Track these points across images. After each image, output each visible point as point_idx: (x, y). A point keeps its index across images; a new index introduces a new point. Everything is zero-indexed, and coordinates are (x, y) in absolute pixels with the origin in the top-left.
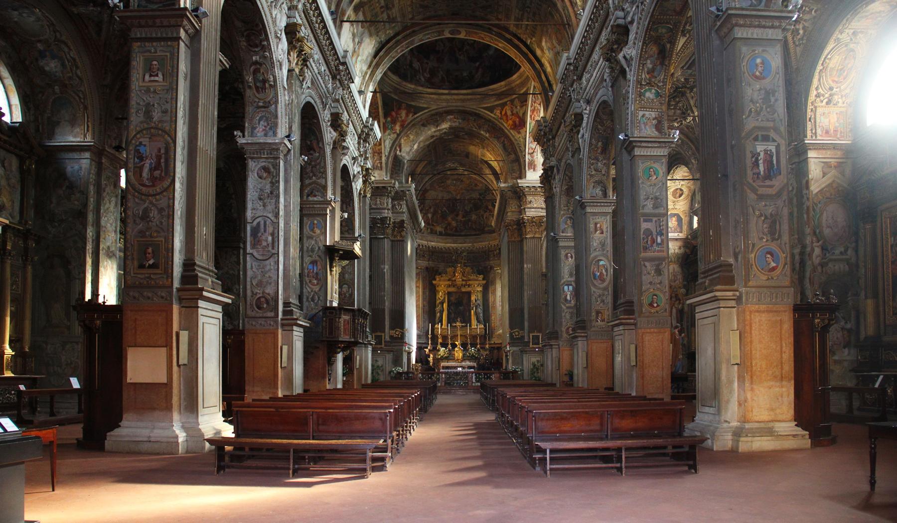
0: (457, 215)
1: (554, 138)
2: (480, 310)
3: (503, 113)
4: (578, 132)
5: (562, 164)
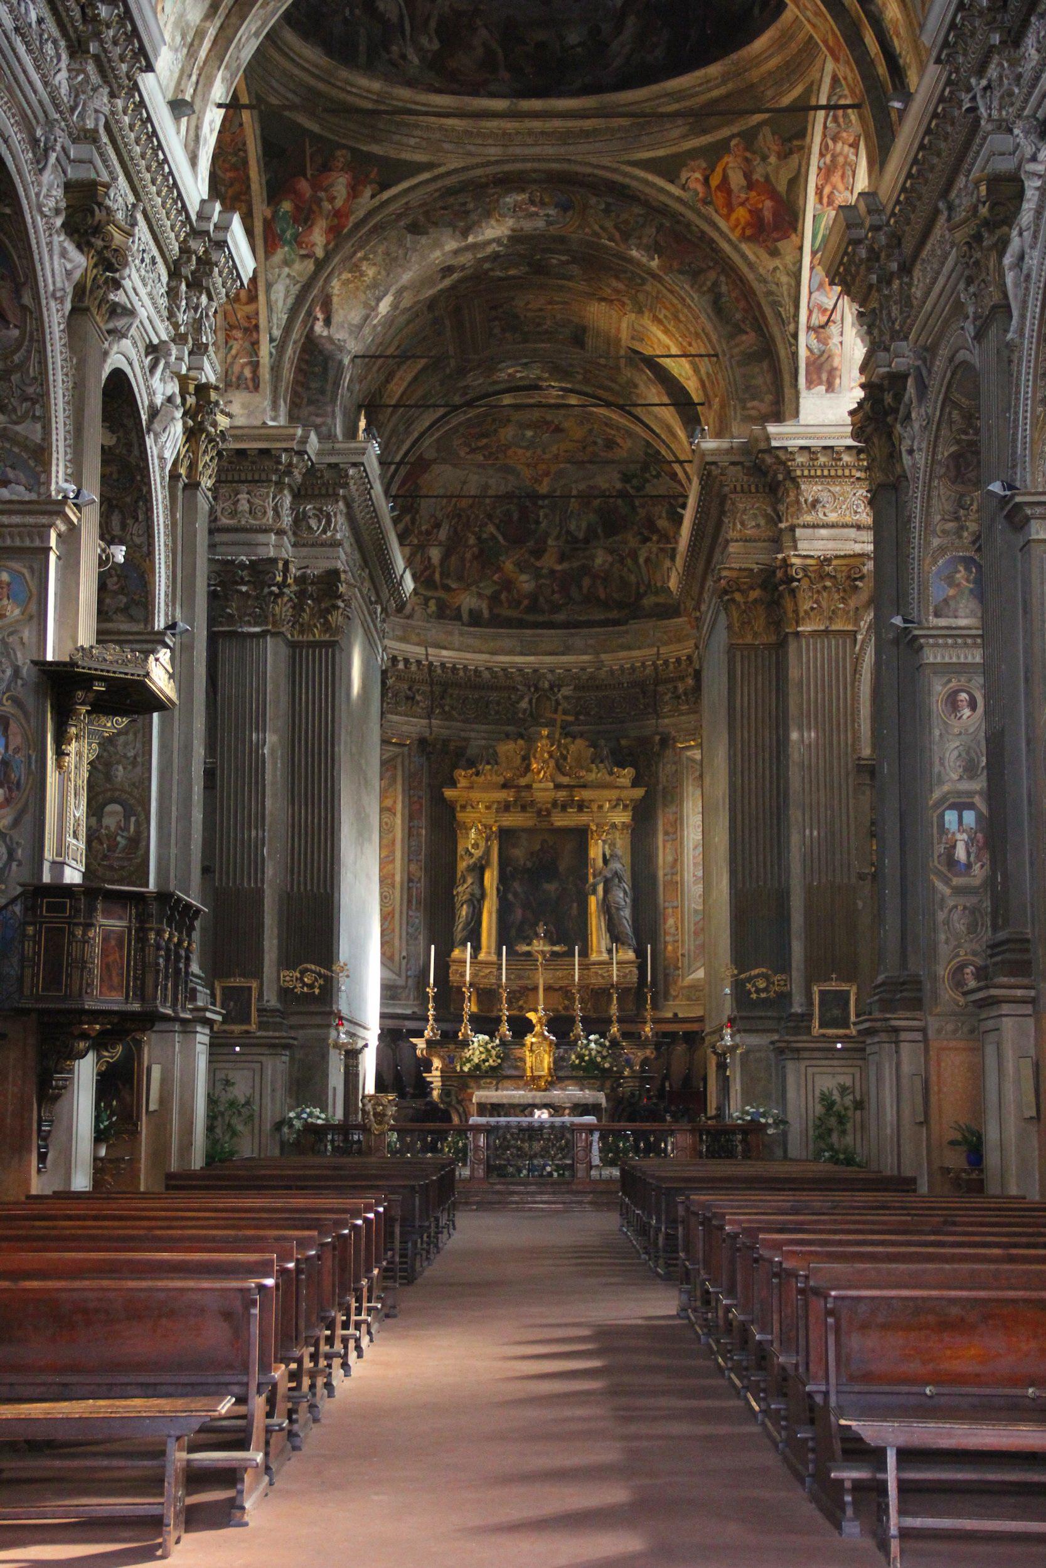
0: (538, 553)
1: (906, 269)
2: (621, 896)
3: (715, 182)
4: (1002, 245)
5: (939, 364)
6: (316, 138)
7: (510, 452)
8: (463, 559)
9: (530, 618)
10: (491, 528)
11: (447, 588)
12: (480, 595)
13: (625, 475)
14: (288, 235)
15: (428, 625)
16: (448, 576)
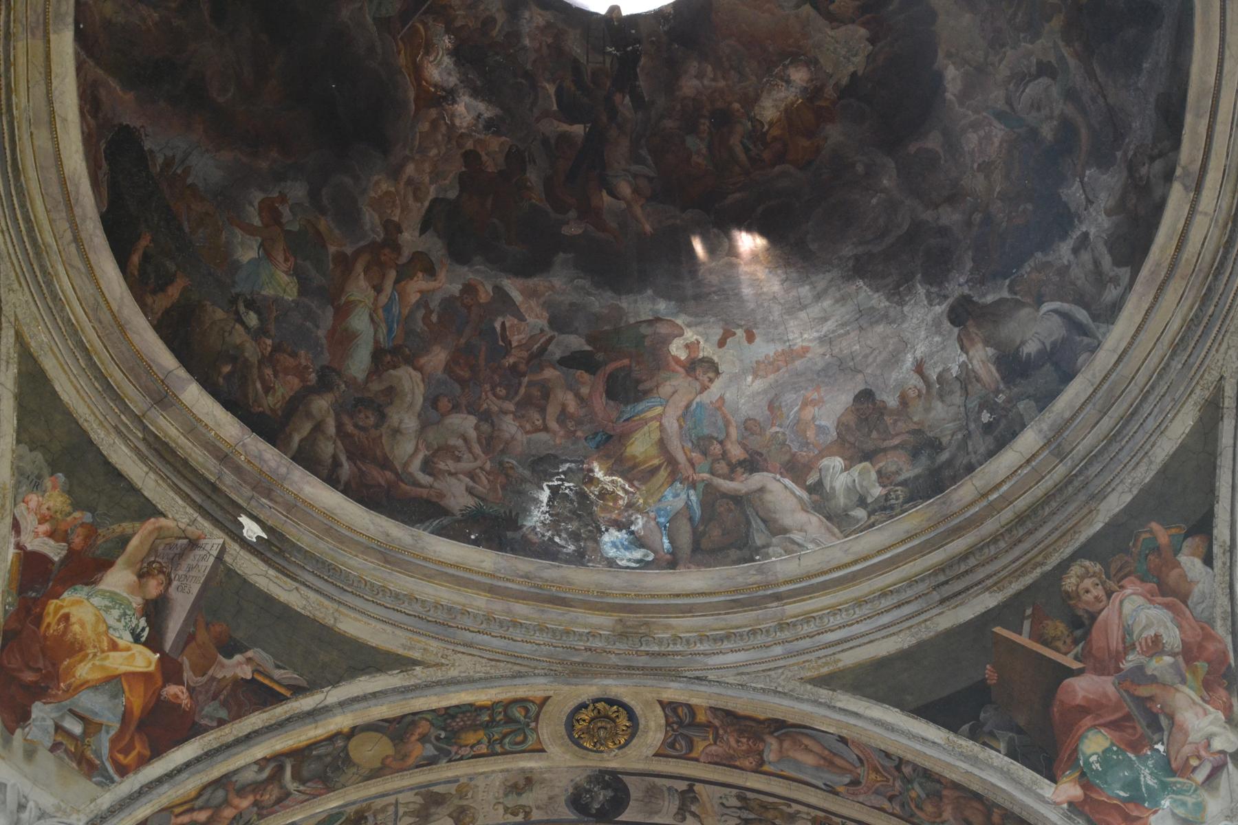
6: (1007, 612)
14: (1148, 779)
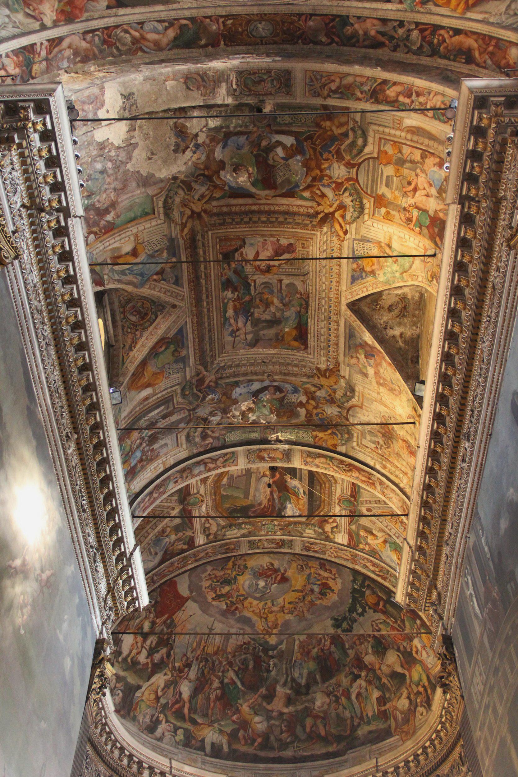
0: (270, 697)
7: (246, 603)
8: (208, 699)
9: (262, 754)
10: (231, 674)
11: (194, 722)
12: (221, 732)
13: (336, 620)
15: (176, 751)
16: (195, 712)
